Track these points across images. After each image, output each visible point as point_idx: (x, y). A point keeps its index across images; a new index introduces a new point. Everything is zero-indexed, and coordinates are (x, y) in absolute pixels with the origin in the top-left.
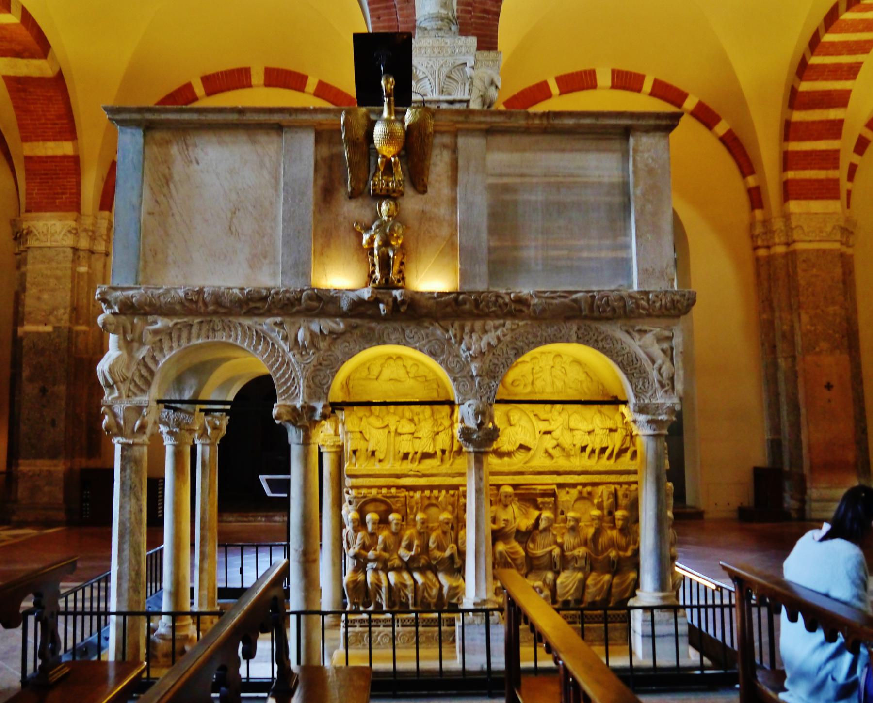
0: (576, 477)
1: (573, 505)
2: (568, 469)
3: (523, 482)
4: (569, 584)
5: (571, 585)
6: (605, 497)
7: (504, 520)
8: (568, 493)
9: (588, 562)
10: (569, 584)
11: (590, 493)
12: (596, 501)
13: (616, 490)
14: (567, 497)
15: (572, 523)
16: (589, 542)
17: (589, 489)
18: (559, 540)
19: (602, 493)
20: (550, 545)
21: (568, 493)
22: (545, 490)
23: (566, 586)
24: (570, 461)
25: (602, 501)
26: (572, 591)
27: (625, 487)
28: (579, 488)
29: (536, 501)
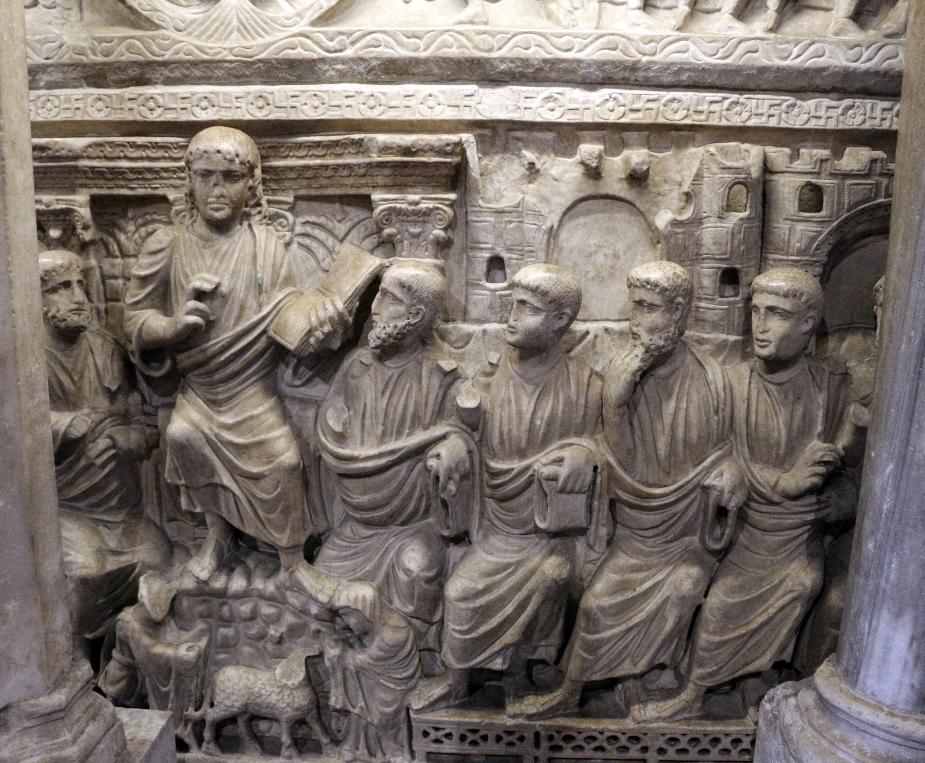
0: (576, 95)
1: (552, 234)
2: (536, 53)
3: (309, 113)
4: (502, 601)
5: (509, 609)
6: (710, 199)
7: (200, 295)
8: (533, 171)
9: (601, 507)
10: (502, 601)
11: (637, 179)
12: (663, 219)
13: (767, 169)
14: (530, 194)
15: (531, 321)
16: (610, 415)
17: (637, 156)
18: (468, 402)
19: (698, 177)
20: (417, 422)
21: (533, 171)
22: (407, 151)
23: (485, 612)
24: (549, 16)
25: (697, 221)
26: (511, 635)
27: (811, 154)
28: (589, 149)
29: (365, 202)
